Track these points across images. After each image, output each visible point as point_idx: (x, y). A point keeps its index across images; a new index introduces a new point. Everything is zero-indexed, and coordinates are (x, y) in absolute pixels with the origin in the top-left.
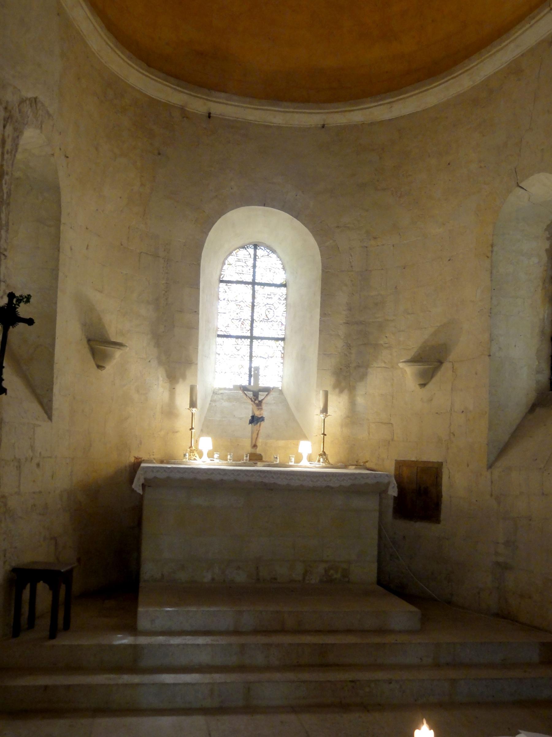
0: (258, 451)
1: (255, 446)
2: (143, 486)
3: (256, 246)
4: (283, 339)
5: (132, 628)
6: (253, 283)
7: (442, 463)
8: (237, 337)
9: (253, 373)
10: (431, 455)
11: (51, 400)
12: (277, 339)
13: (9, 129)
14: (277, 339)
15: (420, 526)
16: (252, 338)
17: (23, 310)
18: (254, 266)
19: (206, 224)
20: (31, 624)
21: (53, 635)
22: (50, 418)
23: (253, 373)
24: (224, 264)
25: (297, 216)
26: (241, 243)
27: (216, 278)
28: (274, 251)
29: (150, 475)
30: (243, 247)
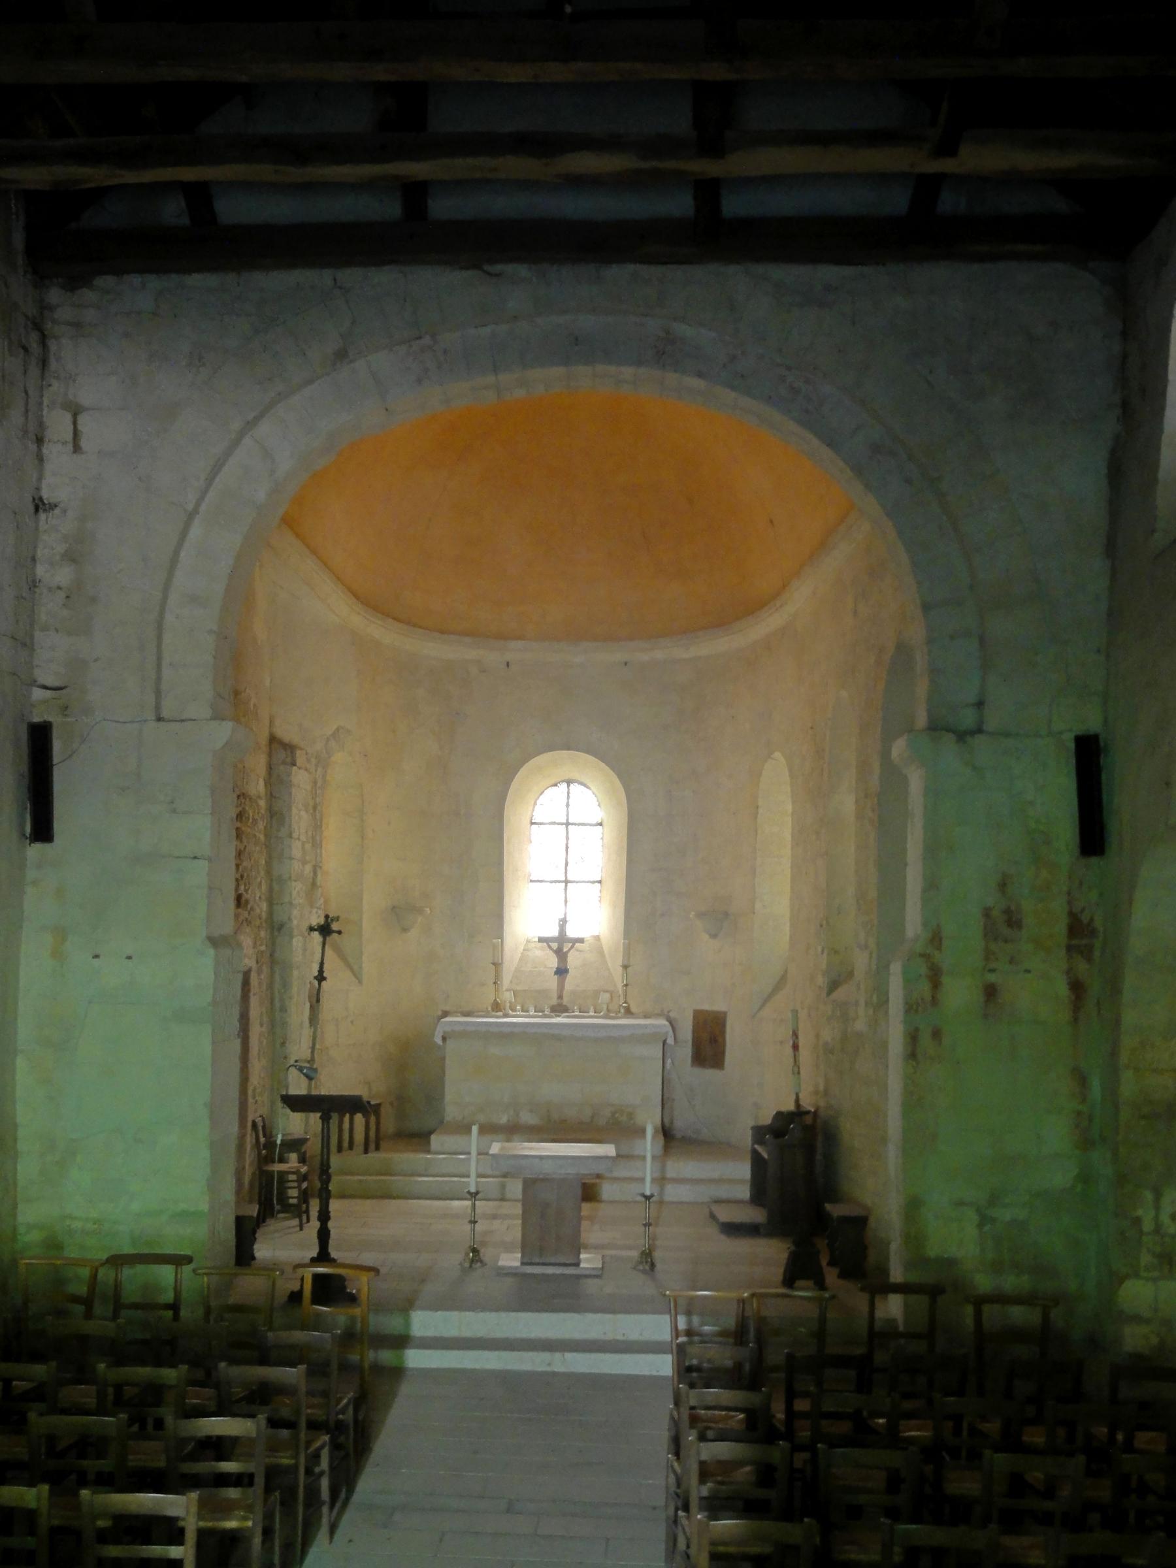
0: (565, 1001)
1: (560, 997)
2: (444, 1039)
3: (569, 782)
4: (600, 882)
5: (429, 1152)
6: (567, 824)
7: (725, 1013)
8: (551, 882)
9: (563, 922)
10: (719, 1006)
11: (361, 967)
12: (594, 882)
13: (320, 770)
14: (594, 882)
15: (709, 1073)
16: (566, 882)
17: (335, 926)
18: (568, 805)
19: (507, 774)
20: (351, 1147)
21: (366, 1151)
22: (360, 982)
23: (563, 922)
24: (535, 804)
25: (602, 758)
26: (553, 782)
27: (527, 821)
28: (588, 788)
29: (448, 1029)
30: (556, 785)
